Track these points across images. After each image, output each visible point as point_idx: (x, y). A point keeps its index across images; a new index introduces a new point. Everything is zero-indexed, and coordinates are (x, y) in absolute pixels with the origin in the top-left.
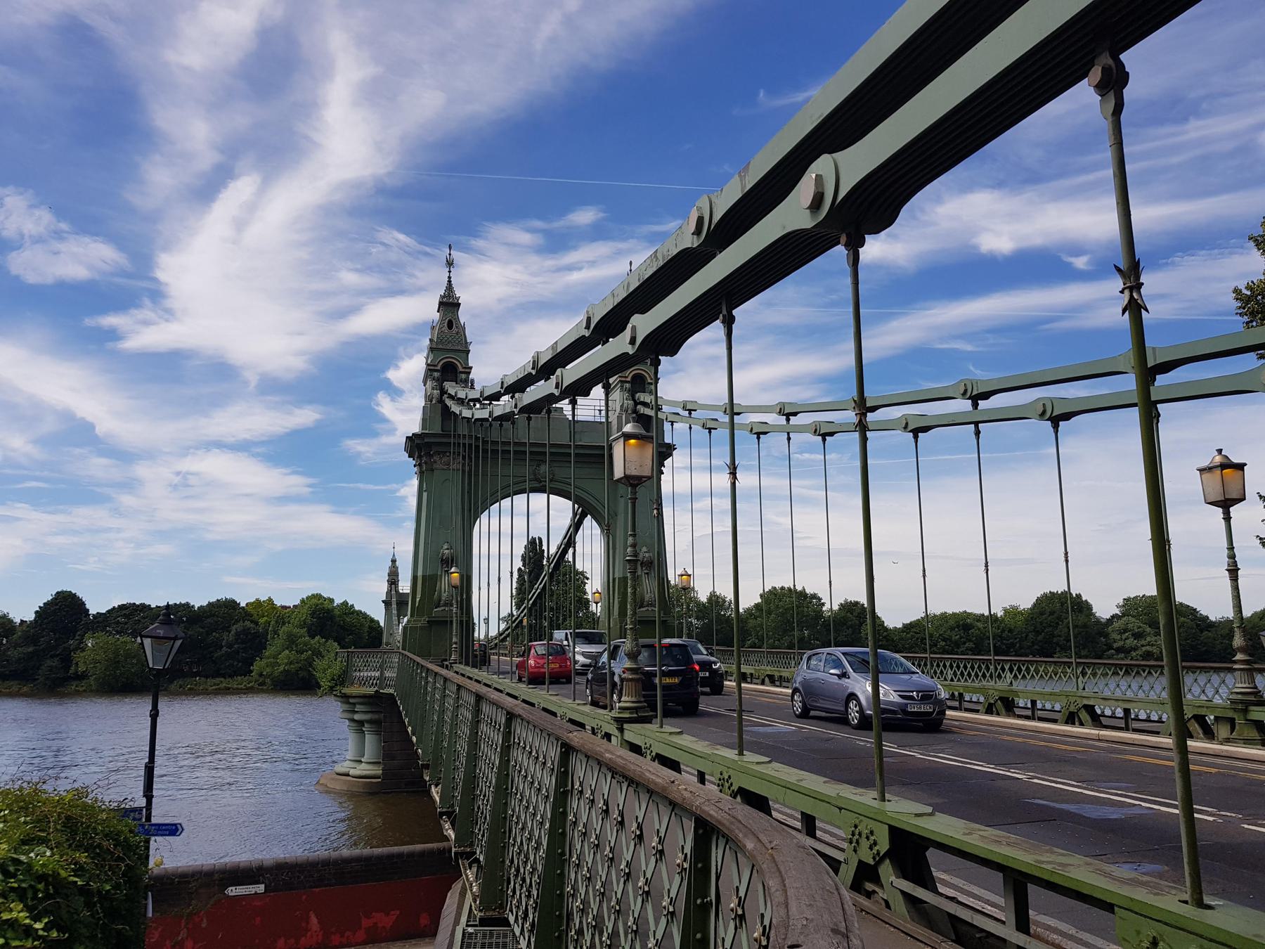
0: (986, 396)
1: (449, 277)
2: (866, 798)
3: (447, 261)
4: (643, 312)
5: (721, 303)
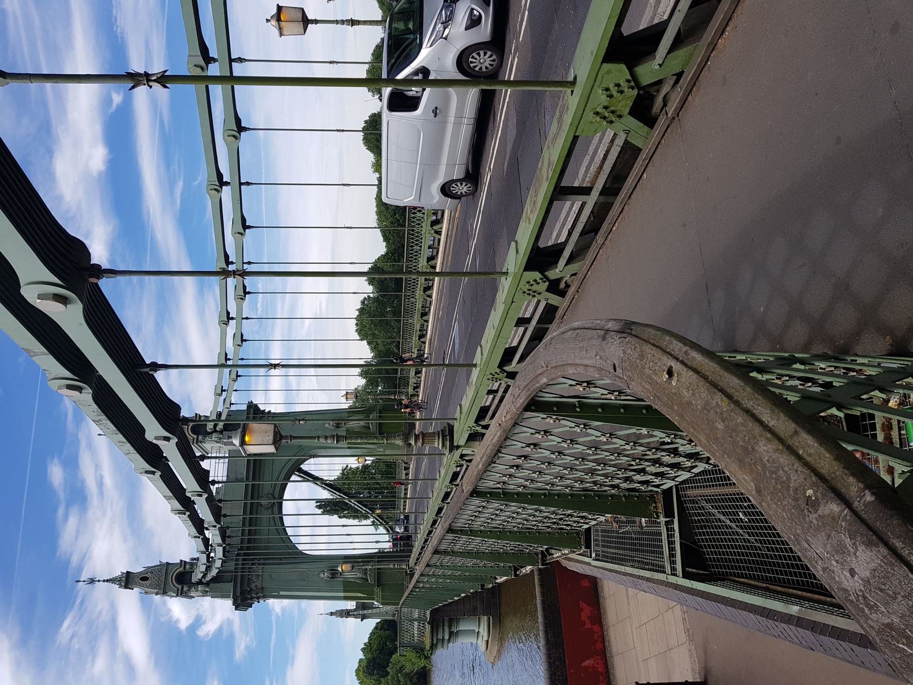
0: (220, 176)
1: (104, 581)
2: (505, 285)
3: (90, 583)
4: (144, 431)
5: (140, 372)
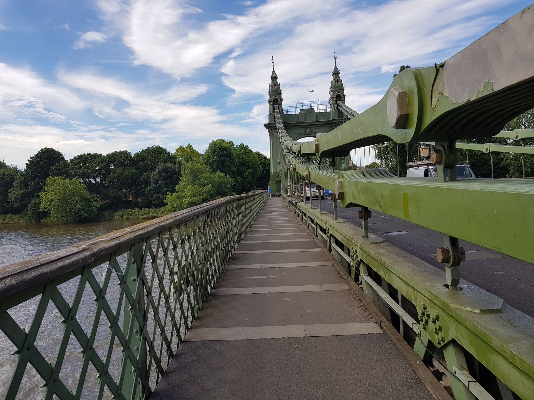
1: (273, 68)
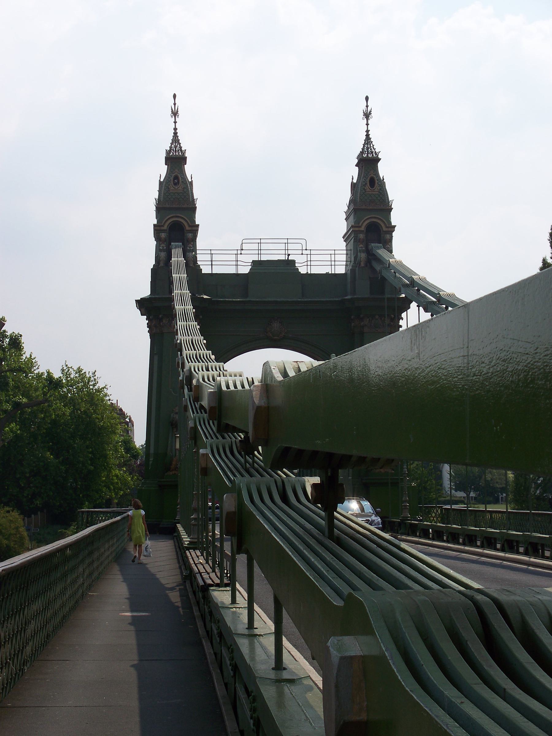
1: (175, 129)
